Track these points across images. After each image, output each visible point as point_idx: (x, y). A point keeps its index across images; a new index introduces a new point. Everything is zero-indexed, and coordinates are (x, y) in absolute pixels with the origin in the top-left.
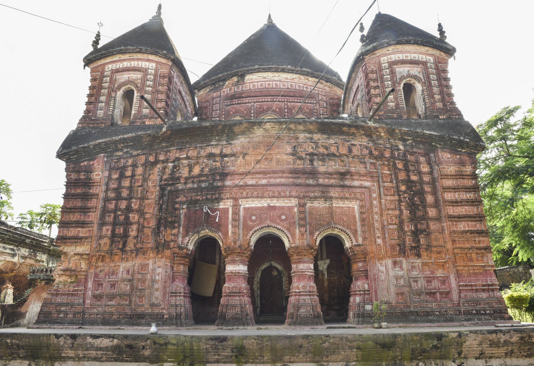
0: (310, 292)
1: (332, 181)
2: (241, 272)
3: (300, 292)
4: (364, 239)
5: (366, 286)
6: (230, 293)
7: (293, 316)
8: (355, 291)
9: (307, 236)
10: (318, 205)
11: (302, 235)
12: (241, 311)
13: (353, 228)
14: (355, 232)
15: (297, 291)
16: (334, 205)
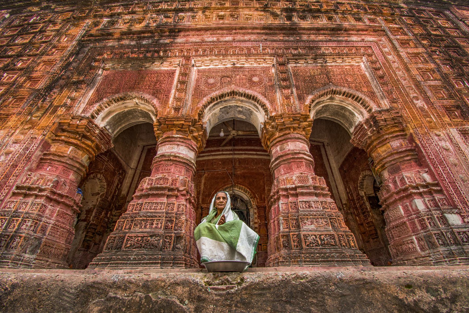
0: (315, 188)
1: (321, 38)
2: (181, 156)
3: (295, 189)
4: (393, 101)
5: (427, 177)
6: (151, 189)
7: (288, 241)
8: (406, 190)
9: (294, 100)
10: (305, 65)
11: (287, 98)
12: (166, 228)
13: (366, 90)
14: (372, 95)
15: (288, 186)
16: (328, 64)
